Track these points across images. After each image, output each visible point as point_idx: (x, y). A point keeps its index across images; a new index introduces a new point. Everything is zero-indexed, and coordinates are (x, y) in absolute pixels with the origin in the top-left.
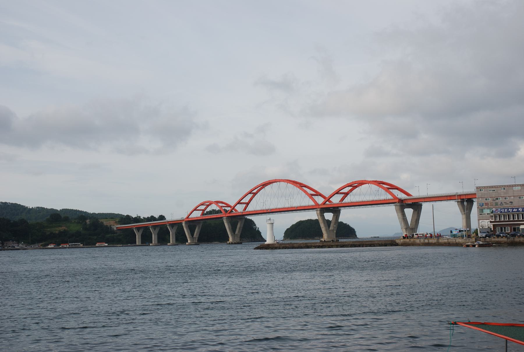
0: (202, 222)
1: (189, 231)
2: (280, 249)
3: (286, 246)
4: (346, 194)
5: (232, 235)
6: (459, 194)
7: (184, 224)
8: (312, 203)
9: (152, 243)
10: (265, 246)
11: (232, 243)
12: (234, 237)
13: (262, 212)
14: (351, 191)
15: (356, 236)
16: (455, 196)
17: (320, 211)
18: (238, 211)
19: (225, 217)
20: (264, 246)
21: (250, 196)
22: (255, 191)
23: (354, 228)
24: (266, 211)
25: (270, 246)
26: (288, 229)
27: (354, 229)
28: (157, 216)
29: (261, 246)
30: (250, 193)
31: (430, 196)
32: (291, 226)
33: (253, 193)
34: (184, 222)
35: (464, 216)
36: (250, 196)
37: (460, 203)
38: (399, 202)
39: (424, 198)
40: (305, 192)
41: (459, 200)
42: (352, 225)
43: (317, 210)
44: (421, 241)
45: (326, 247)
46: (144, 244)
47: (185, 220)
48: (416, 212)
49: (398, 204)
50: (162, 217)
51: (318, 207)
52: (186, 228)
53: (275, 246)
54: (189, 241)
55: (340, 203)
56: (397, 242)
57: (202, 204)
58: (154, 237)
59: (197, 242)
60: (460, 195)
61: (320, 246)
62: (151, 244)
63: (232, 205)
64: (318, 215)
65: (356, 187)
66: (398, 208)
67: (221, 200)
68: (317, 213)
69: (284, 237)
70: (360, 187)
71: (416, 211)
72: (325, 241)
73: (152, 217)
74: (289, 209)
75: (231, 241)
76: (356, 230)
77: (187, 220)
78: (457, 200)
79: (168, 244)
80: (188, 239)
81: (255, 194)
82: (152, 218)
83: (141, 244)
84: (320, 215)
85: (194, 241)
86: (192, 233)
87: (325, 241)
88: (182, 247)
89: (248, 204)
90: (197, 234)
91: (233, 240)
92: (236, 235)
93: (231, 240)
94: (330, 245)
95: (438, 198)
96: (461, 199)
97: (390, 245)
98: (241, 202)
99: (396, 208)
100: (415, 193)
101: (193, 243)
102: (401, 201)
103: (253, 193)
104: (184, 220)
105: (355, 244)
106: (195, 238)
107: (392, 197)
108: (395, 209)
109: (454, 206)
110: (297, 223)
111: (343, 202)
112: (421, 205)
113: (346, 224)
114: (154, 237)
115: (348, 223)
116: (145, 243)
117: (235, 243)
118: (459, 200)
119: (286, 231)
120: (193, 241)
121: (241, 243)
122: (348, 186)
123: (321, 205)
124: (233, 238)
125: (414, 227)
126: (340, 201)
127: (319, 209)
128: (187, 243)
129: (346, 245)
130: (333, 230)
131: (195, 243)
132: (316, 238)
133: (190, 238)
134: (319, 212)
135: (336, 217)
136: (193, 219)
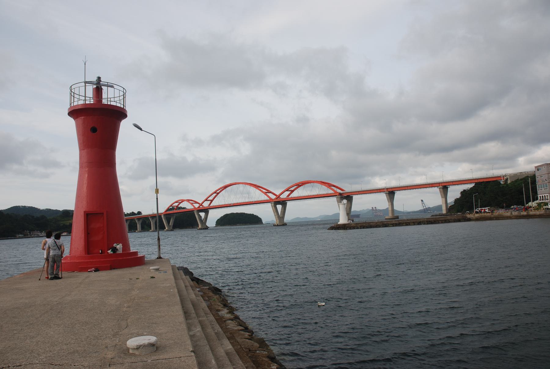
0: (175, 214)
1: (166, 221)
2: (354, 229)
3: (362, 225)
4: (292, 191)
5: (201, 223)
6: (387, 188)
7: (162, 217)
8: (266, 198)
9: (137, 230)
10: (341, 225)
11: (201, 229)
12: (202, 224)
13: (214, 207)
14: (295, 189)
15: (262, 223)
16: (384, 189)
17: (274, 203)
18: (186, 208)
19: (163, 215)
20: (340, 226)
21: (215, 194)
22: (218, 192)
23: (261, 218)
24: (229, 205)
25: (347, 226)
26: (218, 220)
27: (261, 219)
28: (136, 212)
29: (338, 226)
30: (215, 193)
31: (364, 190)
32: (220, 217)
33: (217, 193)
34: (163, 215)
35: (390, 203)
36: (215, 194)
37: (388, 194)
38: (339, 195)
39: (359, 192)
40: (260, 190)
41: (387, 192)
42: (259, 216)
43: (271, 203)
44: (513, 214)
45: (404, 224)
46: (130, 231)
47: (164, 213)
48: (350, 202)
49: (339, 197)
50: (139, 213)
51: (272, 201)
52: (165, 219)
53: (352, 225)
54: (166, 228)
55: (288, 197)
56: (468, 217)
57: (176, 202)
58: (139, 226)
59: (172, 228)
60: (388, 189)
61: (396, 223)
62: (136, 231)
63: (201, 203)
64: (272, 207)
65: (301, 186)
66: (339, 199)
67: (190, 199)
68: (272, 205)
69: (216, 224)
70: (304, 186)
71: (349, 201)
72: (277, 225)
73: (133, 212)
74: (228, 206)
75: (200, 227)
76: (262, 219)
77: (198, 209)
78: (386, 192)
79: (150, 231)
80: (166, 227)
81: (218, 194)
82: (133, 214)
83: (129, 231)
84: (274, 207)
85: (170, 228)
86: (168, 222)
87: (277, 225)
88: (146, 234)
89: (212, 201)
90: (172, 223)
91: (201, 227)
92: (204, 223)
93: (200, 226)
94: (406, 222)
95: (469, 181)
96: (388, 191)
97: (464, 220)
98: (208, 199)
99: (338, 199)
100: (348, 188)
101: (170, 229)
102: (340, 194)
103: (217, 193)
104: (162, 213)
105: (430, 220)
106: (171, 226)
107: (333, 192)
108: (337, 200)
109: (383, 197)
110: (224, 215)
111: (289, 197)
112: (352, 197)
113: (256, 215)
114: (139, 226)
115: (257, 215)
116: (131, 230)
117: (203, 229)
118: (387, 192)
119: (217, 221)
120: (169, 228)
121: (173, 230)
122: (296, 185)
123: (275, 199)
124: (201, 225)
125: (348, 213)
126: (287, 196)
127: (273, 202)
128: (165, 230)
129: (422, 222)
130: (283, 217)
131: (171, 229)
132: (238, 225)
133: (167, 226)
134: (273, 204)
135: (284, 207)
136: (190, 210)
